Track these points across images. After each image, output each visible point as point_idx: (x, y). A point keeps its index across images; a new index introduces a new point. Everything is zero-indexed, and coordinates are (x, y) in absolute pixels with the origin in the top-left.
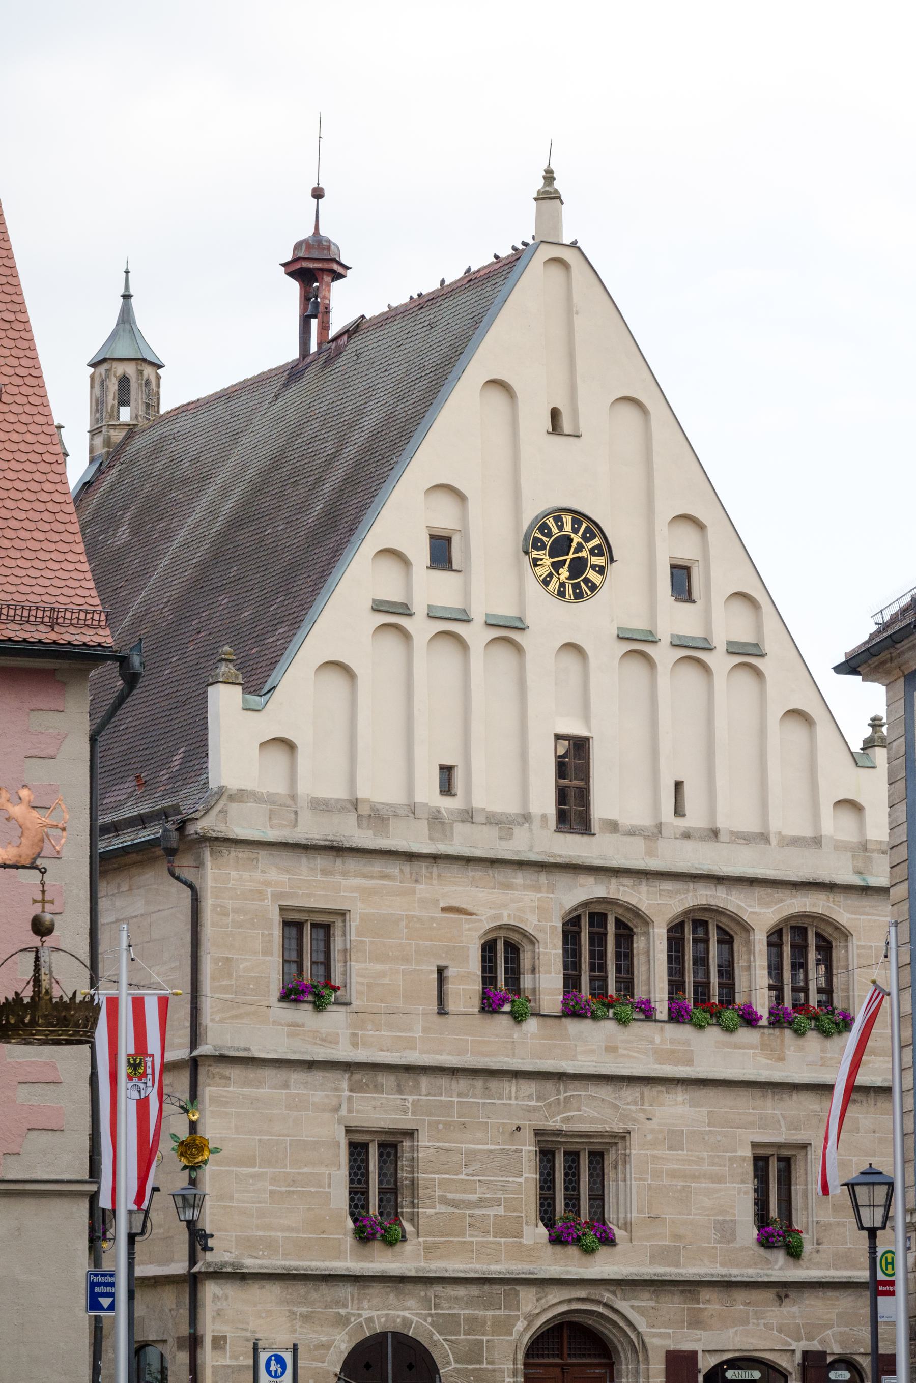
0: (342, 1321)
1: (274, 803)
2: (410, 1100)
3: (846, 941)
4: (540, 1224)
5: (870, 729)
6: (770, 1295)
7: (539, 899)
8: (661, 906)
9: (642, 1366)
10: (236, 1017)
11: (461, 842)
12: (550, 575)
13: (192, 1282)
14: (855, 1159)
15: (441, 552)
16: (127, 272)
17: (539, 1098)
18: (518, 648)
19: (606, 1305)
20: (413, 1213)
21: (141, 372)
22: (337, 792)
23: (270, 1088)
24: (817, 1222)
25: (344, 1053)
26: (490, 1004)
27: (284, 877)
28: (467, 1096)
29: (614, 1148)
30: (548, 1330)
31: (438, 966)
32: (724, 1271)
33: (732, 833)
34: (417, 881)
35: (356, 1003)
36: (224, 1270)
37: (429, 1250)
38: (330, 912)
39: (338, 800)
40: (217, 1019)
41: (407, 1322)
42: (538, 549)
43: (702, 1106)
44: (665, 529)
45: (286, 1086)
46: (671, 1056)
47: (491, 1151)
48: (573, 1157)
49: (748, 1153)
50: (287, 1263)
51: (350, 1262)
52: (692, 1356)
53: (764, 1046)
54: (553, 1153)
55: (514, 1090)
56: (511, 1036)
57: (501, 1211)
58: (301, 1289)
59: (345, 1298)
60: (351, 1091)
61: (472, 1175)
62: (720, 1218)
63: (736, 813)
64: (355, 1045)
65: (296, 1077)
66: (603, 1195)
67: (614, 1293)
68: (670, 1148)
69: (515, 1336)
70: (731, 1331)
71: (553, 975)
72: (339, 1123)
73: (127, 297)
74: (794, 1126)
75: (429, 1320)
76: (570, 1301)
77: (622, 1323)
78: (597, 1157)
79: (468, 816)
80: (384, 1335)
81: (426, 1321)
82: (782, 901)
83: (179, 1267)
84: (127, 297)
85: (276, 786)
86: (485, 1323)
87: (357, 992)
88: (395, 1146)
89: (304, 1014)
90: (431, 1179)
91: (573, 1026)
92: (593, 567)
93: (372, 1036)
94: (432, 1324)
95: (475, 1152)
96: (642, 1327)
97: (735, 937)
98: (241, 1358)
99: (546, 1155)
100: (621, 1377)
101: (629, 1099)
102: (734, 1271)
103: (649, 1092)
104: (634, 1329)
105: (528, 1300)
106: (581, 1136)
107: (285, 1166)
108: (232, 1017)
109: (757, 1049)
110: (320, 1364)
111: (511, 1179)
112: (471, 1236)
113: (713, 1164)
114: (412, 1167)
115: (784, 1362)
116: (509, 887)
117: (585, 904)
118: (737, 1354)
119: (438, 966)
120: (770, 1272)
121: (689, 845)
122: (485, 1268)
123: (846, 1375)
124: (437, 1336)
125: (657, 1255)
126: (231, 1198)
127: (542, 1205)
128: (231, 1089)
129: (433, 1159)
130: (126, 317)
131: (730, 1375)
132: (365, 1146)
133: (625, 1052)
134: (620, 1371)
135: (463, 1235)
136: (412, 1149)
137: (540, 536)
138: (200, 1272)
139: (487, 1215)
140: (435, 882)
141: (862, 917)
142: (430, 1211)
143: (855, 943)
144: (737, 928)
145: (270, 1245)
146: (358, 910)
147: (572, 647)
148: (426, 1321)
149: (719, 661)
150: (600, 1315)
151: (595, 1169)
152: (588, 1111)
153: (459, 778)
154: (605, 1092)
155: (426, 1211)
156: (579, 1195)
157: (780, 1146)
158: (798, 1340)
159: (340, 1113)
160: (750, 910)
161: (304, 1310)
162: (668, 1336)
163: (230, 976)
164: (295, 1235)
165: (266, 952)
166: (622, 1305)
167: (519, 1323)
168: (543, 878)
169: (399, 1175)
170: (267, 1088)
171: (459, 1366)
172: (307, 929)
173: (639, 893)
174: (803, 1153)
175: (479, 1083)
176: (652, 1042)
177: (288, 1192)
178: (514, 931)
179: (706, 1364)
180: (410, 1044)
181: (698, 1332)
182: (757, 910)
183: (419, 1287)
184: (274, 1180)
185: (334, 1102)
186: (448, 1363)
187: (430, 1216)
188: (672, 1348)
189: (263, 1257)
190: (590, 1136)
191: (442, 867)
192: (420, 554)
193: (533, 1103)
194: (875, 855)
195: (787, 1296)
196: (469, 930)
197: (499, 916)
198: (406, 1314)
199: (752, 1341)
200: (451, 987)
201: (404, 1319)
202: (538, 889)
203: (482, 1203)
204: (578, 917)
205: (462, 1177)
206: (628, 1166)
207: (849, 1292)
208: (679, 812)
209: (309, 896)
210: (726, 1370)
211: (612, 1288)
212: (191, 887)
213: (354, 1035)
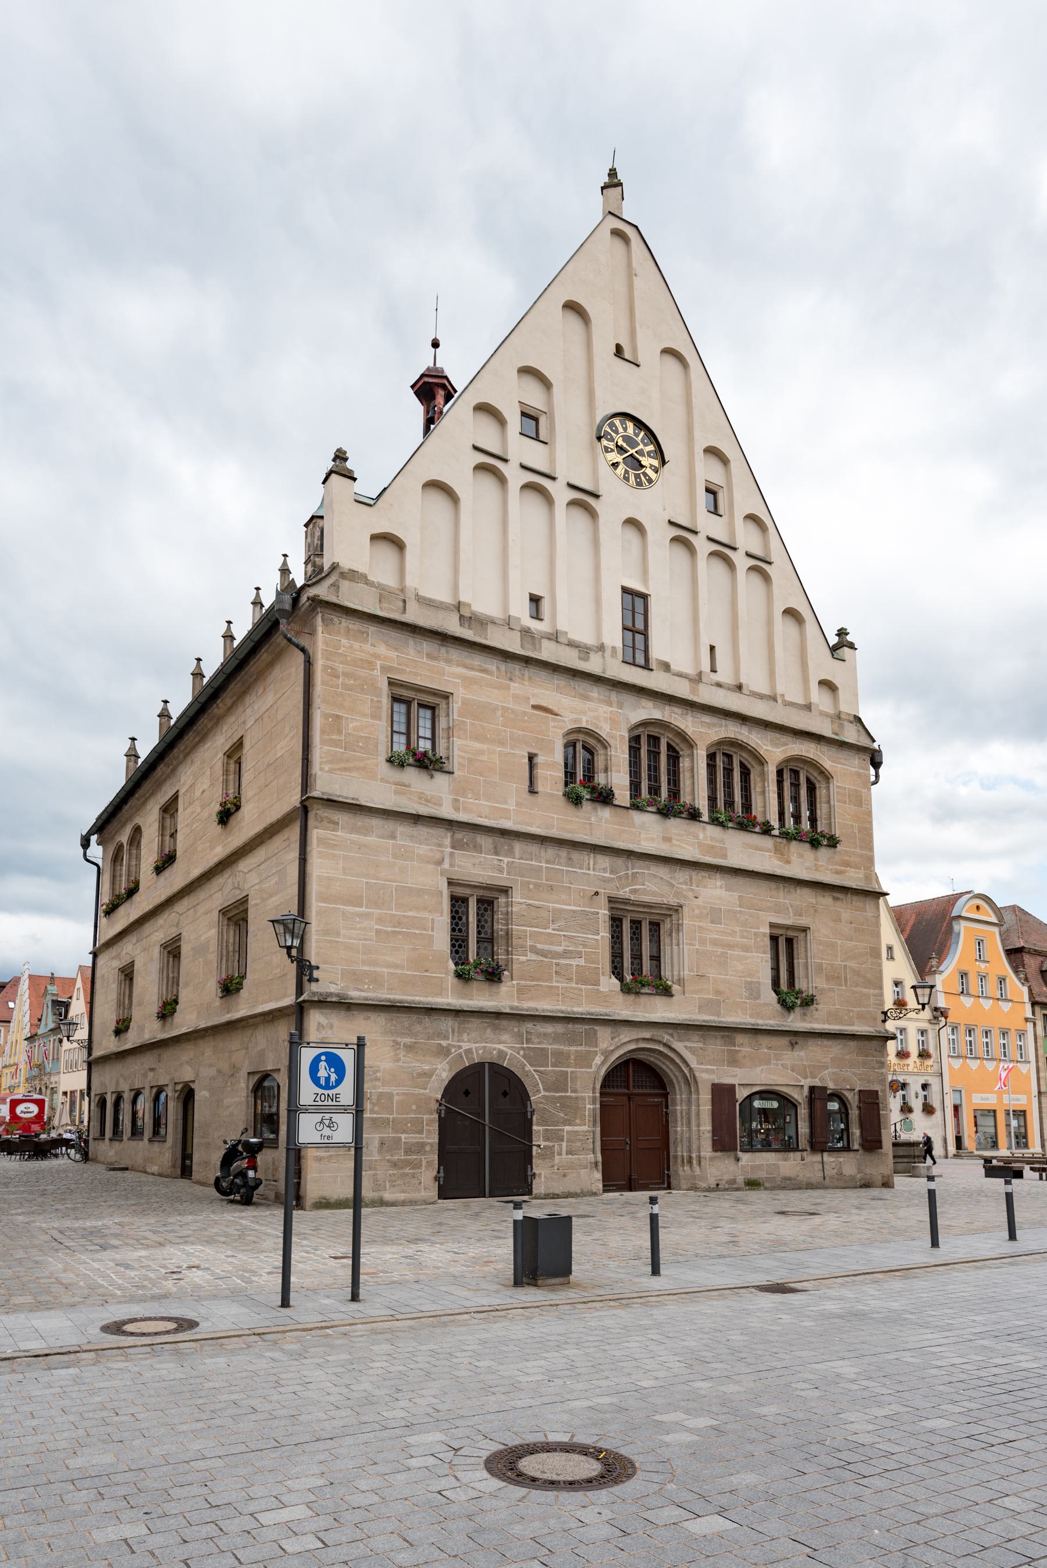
0: (444, 1052)
6: (784, 1041)
7: (611, 712)
9: (694, 1096)
11: (548, 652)
13: (300, 1010)
17: (612, 872)
18: (592, 513)
19: (665, 1045)
22: (443, 596)
23: (377, 837)
25: (446, 812)
28: (553, 863)
31: (529, 753)
32: (753, 1021)
34: (511, 679)
35: (457, 773)
36: (329, 999)
38: (435, 693)
41: (502, 1054)
45: (393, 836)
46: (710, 849)
47: (574, 911)
48: (636, 924)
49: (767, 930)
50: (392, 997)
51: (450, 997)
52: (731, 1088)
53: (777, 850)
54: (621, 920)
56: (589, 819)
57: (582, 962)
58: (405, 1020)
59: (447, 1031)
60: (453, 847)
64: (457, 809)
65: (402, 829)
66: (659, 957)
67: (672, 1036)
68: (712, 922)
69: (594, 1069)
70: (758, 1069)
72: (442, 875)
75: (522, 1053)
76: (637, 1040)
77: (678, 1061)
78: (655, 926)
79: (554, 637)
80: (481, 1065)
89: (412, 776)
90: (523, 931)
91: (637, 817)
93: (472, 803)
94: (523, 1057)
95: (560, 911)
96: (694, 1065)
99: (616, 922)
100: (675, 1104)
101: (681, 880)
102: (760, 1022)
103: (697, 875)
104: (688, 1065)
105: (605, 1038)
106: (644, 906)
107: (391, 909)
110: (422, 1091)
111: (590, 936)
112: (557, 982)
113: (743, 937)
114: (507, 920)
116: (586, 698)
118: (763, 1088)
119: (529, 753)
122: (569, 1009)
124: (528, 1068)
125: (705, 1006)
127: (613, 962)
132: (465, 900)
136: (507, 905)
142: (523, 958)
145: (376, 980)
146: (460, 694)
147: (632, 523)
152: (650, 886)
153: (545, 606)
154: (662, 871)
155: (518, 958)
157: (788, 928)
158: (806, 1078)
161: (408, 1040)
162: (712, 1071)
164: (399, 972)
166: (678, 1046)
167: (597, 1058)
171: (547, 1094)
172: (414, 706)
174: (803, 935)
175: (564, 853)
176: (697, 837)
177: (394, 932)
179: (741, 1094)
181: (735, 1069)
183: (513, 1023)
184: (380, 920)
185: (438, 856)
186: (538, 1091)
187: (522, 963)
189: (368, 990)
193: (607, 875)
195: (796, 1043)
196: (554, 727)
198: (501, 1047)
199: (774, 1077)
200: (540, 772)
201: (500, 1051)
203: (566, 954)
205: (550, 931)
207: (839, 1041)
211: (670, 1031)
213: (456, 800)
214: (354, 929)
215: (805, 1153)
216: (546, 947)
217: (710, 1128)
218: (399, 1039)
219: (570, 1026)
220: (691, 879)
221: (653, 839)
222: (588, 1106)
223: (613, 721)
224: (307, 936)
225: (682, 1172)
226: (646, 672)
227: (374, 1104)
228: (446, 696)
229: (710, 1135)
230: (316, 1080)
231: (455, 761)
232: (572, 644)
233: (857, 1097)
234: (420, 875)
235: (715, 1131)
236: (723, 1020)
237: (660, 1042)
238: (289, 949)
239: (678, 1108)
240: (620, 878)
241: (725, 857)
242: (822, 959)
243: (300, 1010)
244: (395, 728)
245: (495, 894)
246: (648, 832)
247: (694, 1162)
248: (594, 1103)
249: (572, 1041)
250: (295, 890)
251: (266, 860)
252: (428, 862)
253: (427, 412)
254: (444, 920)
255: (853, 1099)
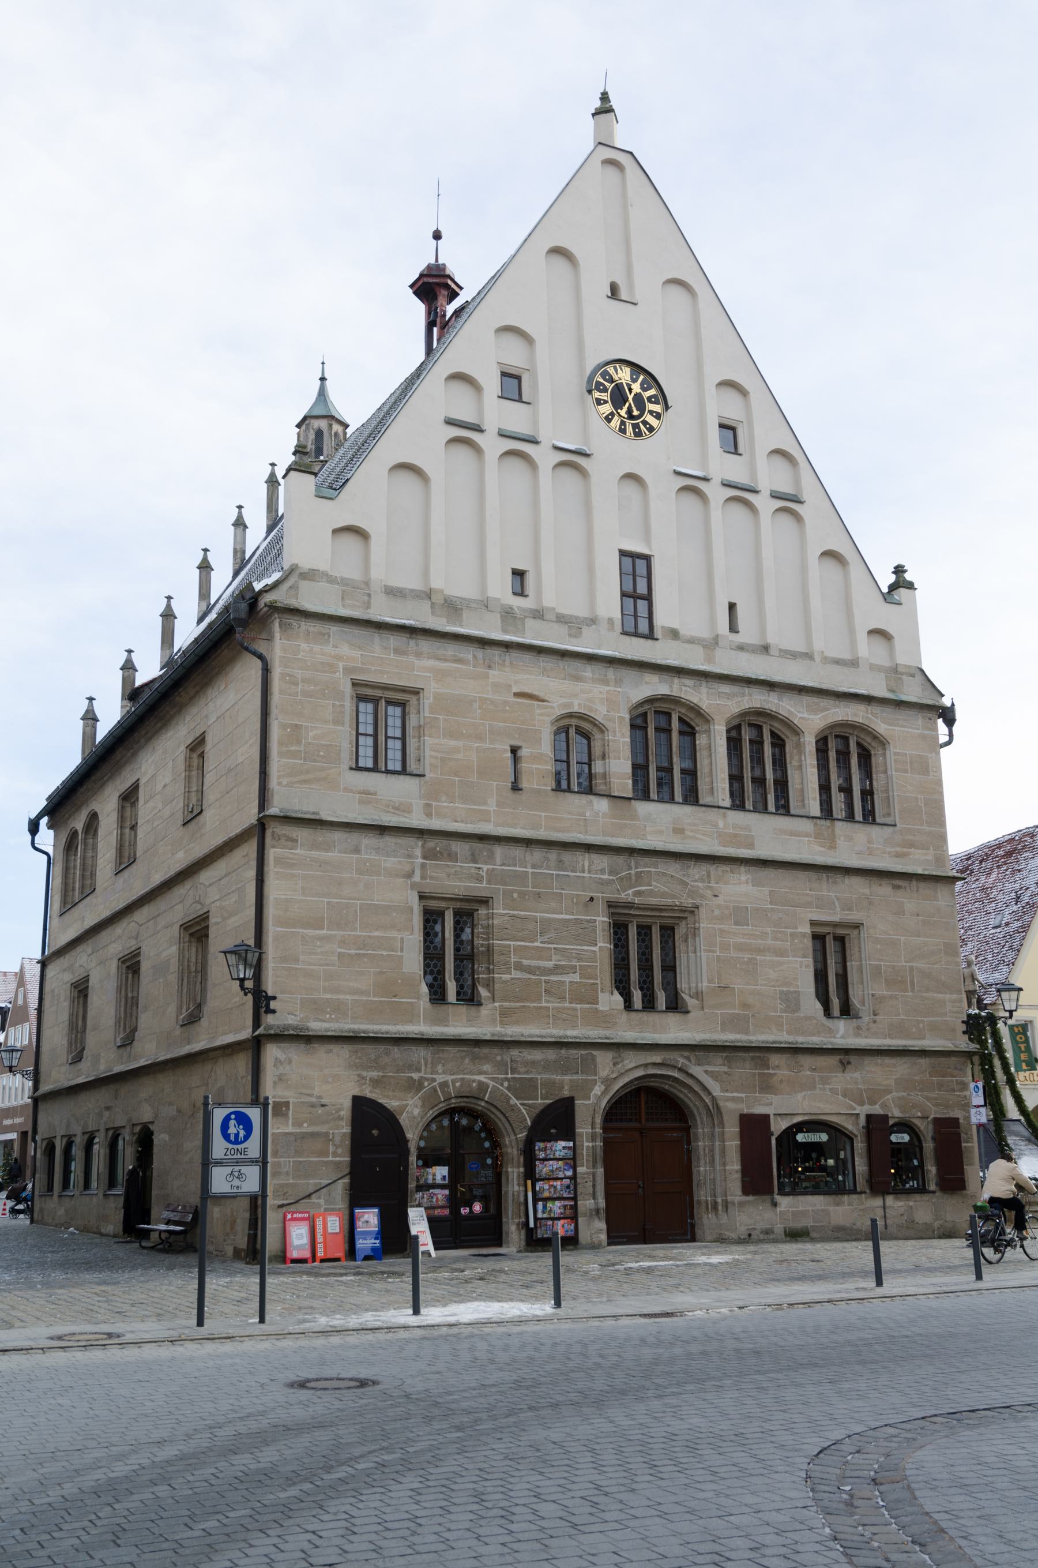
0: (415, 1086)
1: (347, 585)
2: (485, 870)
3: (884, 749)
4: (616, 992)
5: (894, 576)
6: (833, 1061)
7: (607, 692)
8: (721, 706)
9: (717, 1130)
10: (305, 782)
12: (612, 414)
13: (256, 1045)
14: (902, 938)
15: (513, 384)
16: (323, 363)
17: (611, 873)
19: (680, 1070)
20: (488, 979)
21: (331, 426)
23: (339, 852)
24: (873, 995)
25: (417, 820)
26: (562, 785)
27: (356, 654)
28: (541, 867)
29: (684, 922)
30: (626, 1094)
32: (790, 1038)
33: (781, 650)
34: (490, 667)
37: (505, 1015)
39: (412, 591)
40: (285, 783)
42: (600, 391)
43: (764, 886)
44: (714, 389)
45: (357, 850)
46: (734, 839)
47: (566, 921)
48: (644, 931)
49: (807, 929)
52: (764, 1120)
53: (818, 835)
55: (586, 864)
57: (576, 978)
59: (419, 1062)
60: (425, 858)
61: (547, 943)
62: (785, 989)
63: (783, 632)
64: (429, 815)
65: (368, 841)
66: (675, 967)
67: (688, 1059)
68: (736, 923)
69: (592, 1100)
70: (800, 1096)
71: (622, 760)
72: (412, 889)
73: (323, 379)
74: (847, 907)
75: (506, 1084)
76: (646, 1065)
77: (697, 1088)
78: (668, 932)
81: (502, 1085)
82: (827, 709)
83: (246, 1034)
84: (323, 379)
85: (351, 572)
86: (563, 1087)
87: (431, 765)
88: (470, 914)
91: (643, 808)
92: (651, 412)
94: (509, 1088)
97: (787, 741)
98: (305, 1125)
99: (619, 930)
100: (697, 1140)
101: (697, 877)
102: (801, 1039)
103: (714, 870)
104: (710, 1093)
106: (652, 910)
107: (355, 929)
108: (300, 782)
109: (810, 836)
111: (586, 948)
112: (547, 1001)
113: (776, 939)
114: (488, 934)
115: (849, 1126)
116: (578, 679)
117: (650, 700)
118: (806, 1118)
120: (833, 1040)
121: (744, 656)
122: (561, 1033)
123: (906, 1138)
124: (514, 1101)
126: (297, 960)
128: (298, 851)
129: (508, 926)
130: (322, 393)
131: (800, 1137)
133: (692, 834)
134: (696, 1134)
135: (539, 1000)
137: (602, 381)
138: (259, 1035)
139: (563, 982)
140: (507, 669)
141: (897, 728)
143: (892, 750)
144: (788, 733)
145: (338, 1009)
146: (432, 689)
148: (502, 1085)
149: (765, 504)
150: (675, 1079)
151: (667, 942)
152: (657, 886)
154: (673, 868)
156: (652, 966)
157: (835, 925)
158: (862, 1104)
159: (413, 880)
160: (799, 715)
161: (374, 1074)
162: (739, 1100)
163: (299, 742)
164: (365, 998)
165: (337, 722)
166: (697, 1071)
167: (597, 1087)
168: (611, 673)
169: (475, 943)
170: (337, 850)
173: (700, 693)
174: (856, 932)
175: (553, 855)
176: (716, 826)
178: (585, 720)
179: (778, 1126)
180: (485, 816)
182: (805, 715)
183: (496, 1051)
184: (343, 943)
185: (407, 868)
188: (745, 1111)
190: (660, 910)
191: (515, 654)
192: (492, 384)
193: (606, 877)
194: (904, 677)
195: (849, 1063)
196: (541, 715)
197: (571, 705)
198: (482, 1078)
199: (821, 1105)
200: (524, 765)
201: (480, 1083)
202: (605, 682)
203: (558, 970)
204: (645, 714)
206: (697, 939)
207: (905, 1059)
208: (733, 628)
209: (382, 672)
210: (796, 1134)
211: (686, 1054)
212: (261, 657)
214: (315, 954)
215: (863, 1196)
216: (534, 963)
217: (737, 1167)
218: (365, 1074)
219: (563, 1052)
220: (709, 876)
221: (661, 832)
222: (586, 1144)
223: (611, 702)
224: (264, 964)
225: (707, 1221)
226: (650, 642)
227: (336, 1146)
228: (416, 692)
229: (739, 1175)
230: (226, 1136)
231: (427, 762)
232: (561, 619)
233: (931, 1127)
234: (389, 890)
235: (745, 1171)
236: (753, 1038)
237: (674, 1067)
238: (242, 981)
239: (700, 1143)
240: (621, 879)
241: (751, 846)
242: (880, 960)
243: (256, 1045)
244: (361, 731)
245: (475, 906)
246: (659, 823)
247: (720, 1208)
248: (593, 1139)
249: (566, 1068)
250: (251, 912)
251: (226, 875)
252: (397, 876)
253: (429, 313)
254: (415, 938)
255: (926, 1130)
